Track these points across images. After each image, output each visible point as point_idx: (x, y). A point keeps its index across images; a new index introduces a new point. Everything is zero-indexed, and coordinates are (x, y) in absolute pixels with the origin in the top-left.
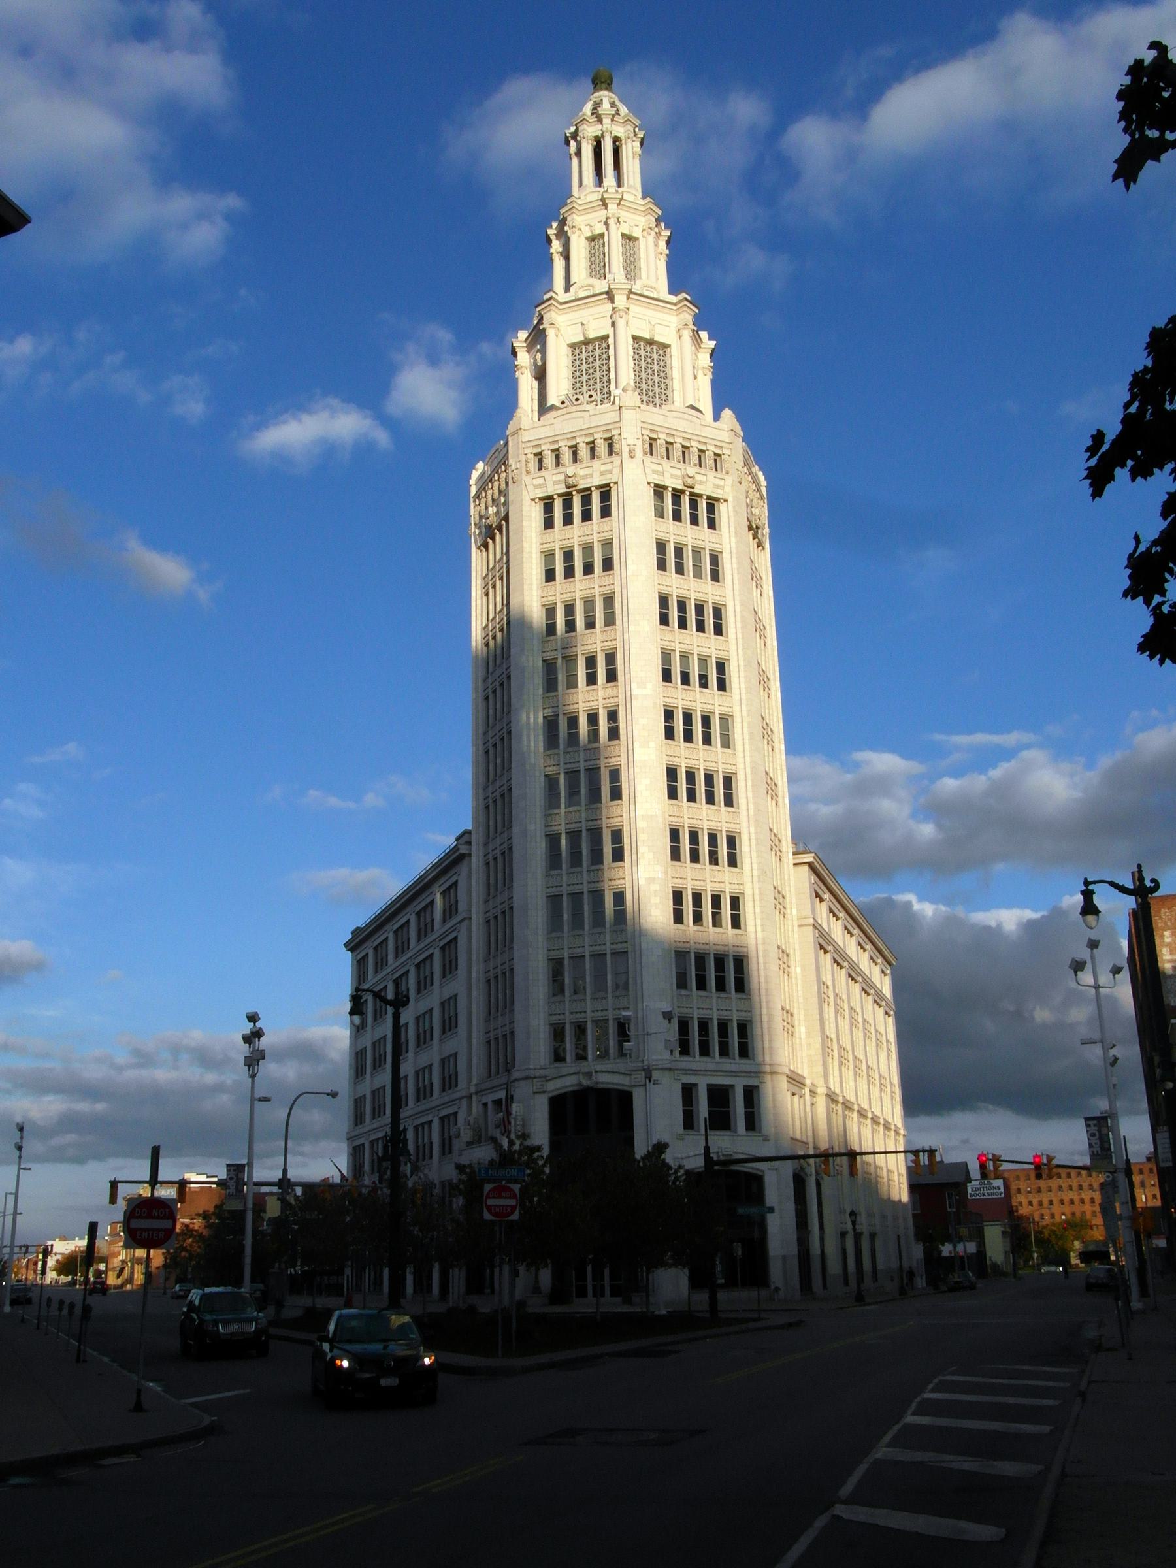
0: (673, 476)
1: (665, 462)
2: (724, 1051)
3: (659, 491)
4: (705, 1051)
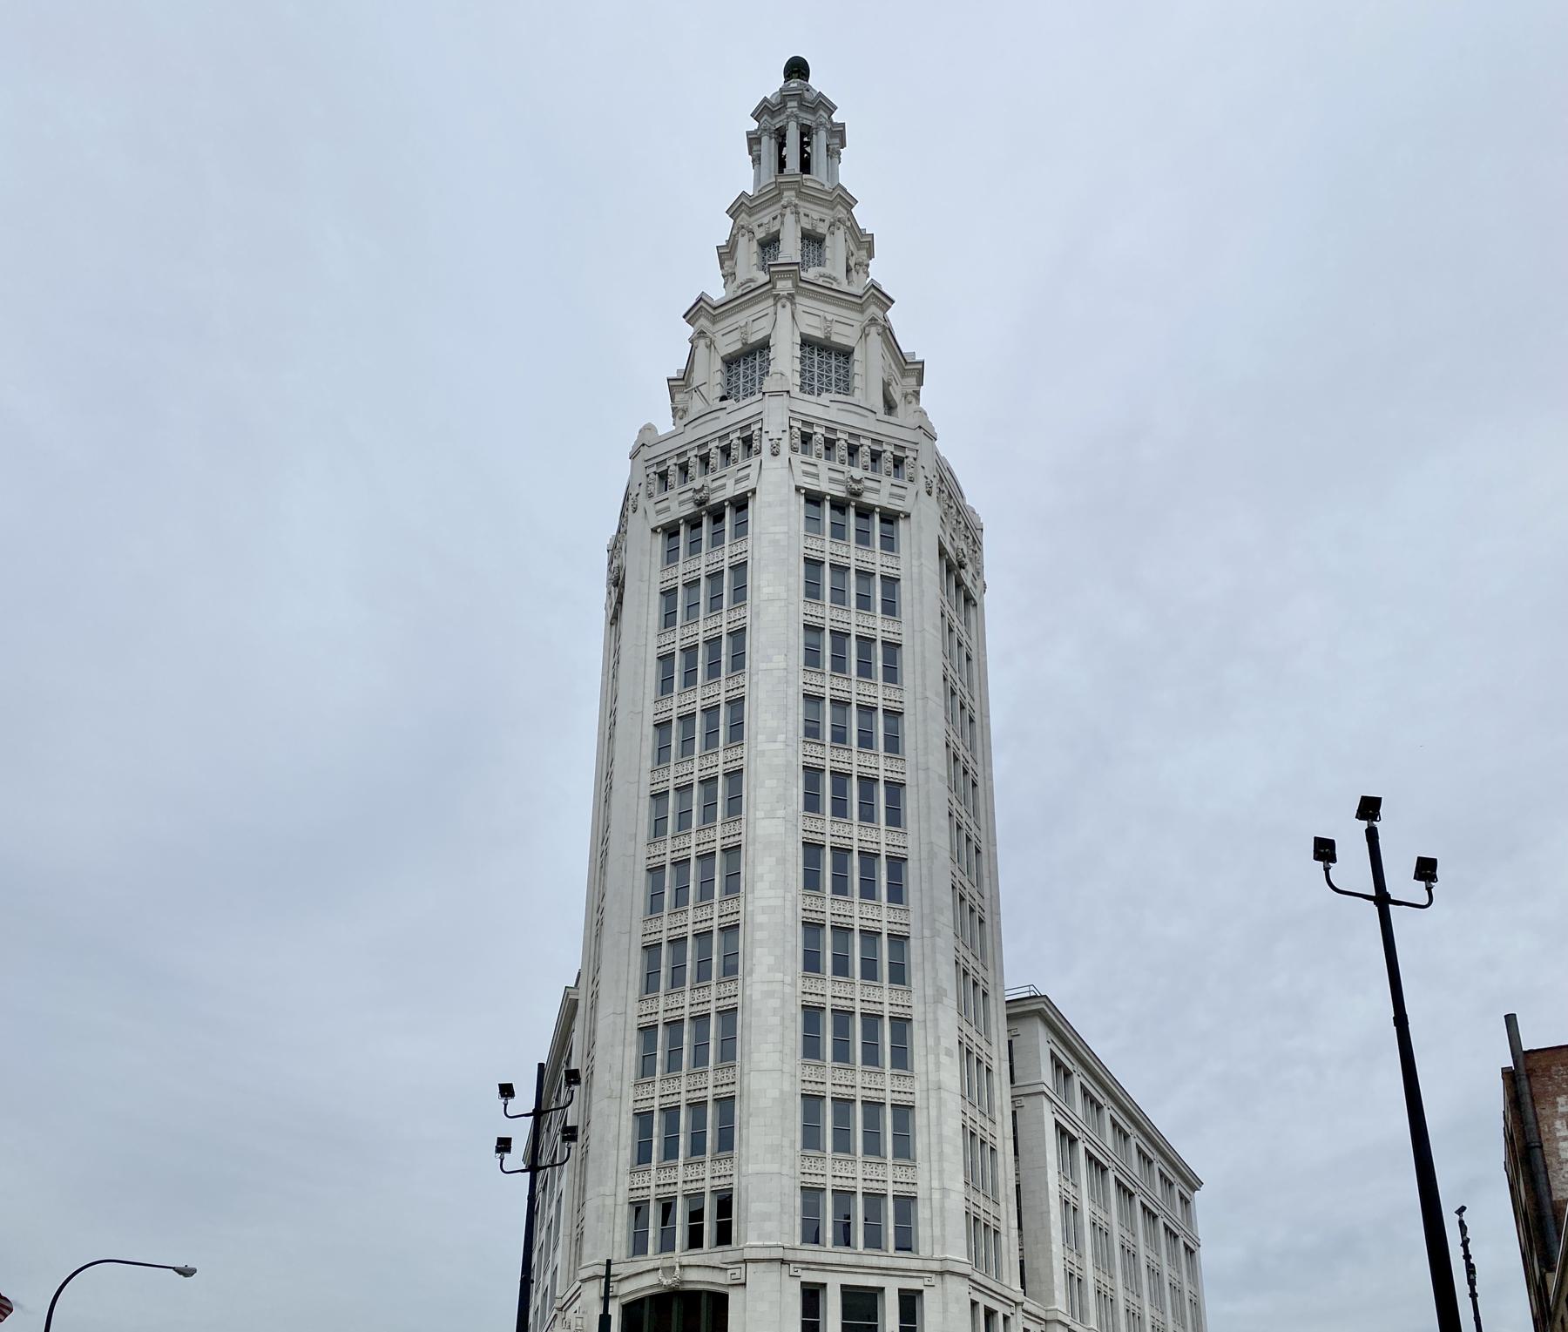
0: (832, 480)
1: (823, 464)
2: (874, 1240)
3: (813, 499)
4: (844, 1237)
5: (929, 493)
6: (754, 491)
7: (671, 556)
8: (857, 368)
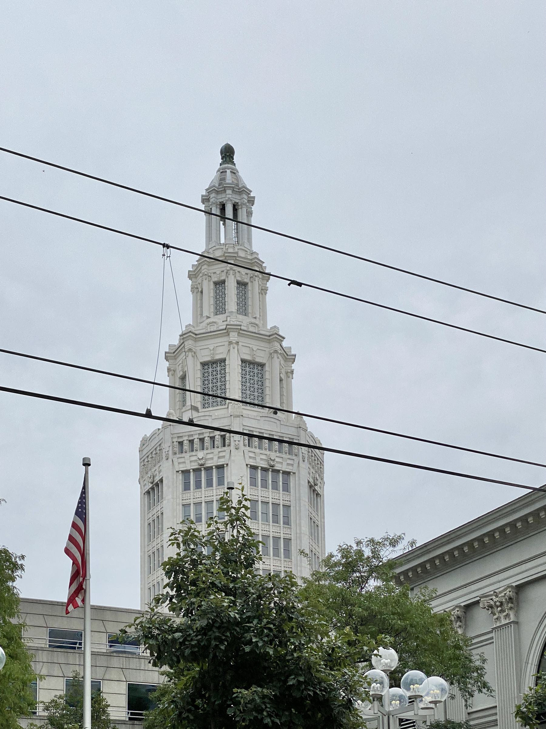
5: (304, 461)
6: (227, 465)
7: (186, 487)
8: (267, 375)
